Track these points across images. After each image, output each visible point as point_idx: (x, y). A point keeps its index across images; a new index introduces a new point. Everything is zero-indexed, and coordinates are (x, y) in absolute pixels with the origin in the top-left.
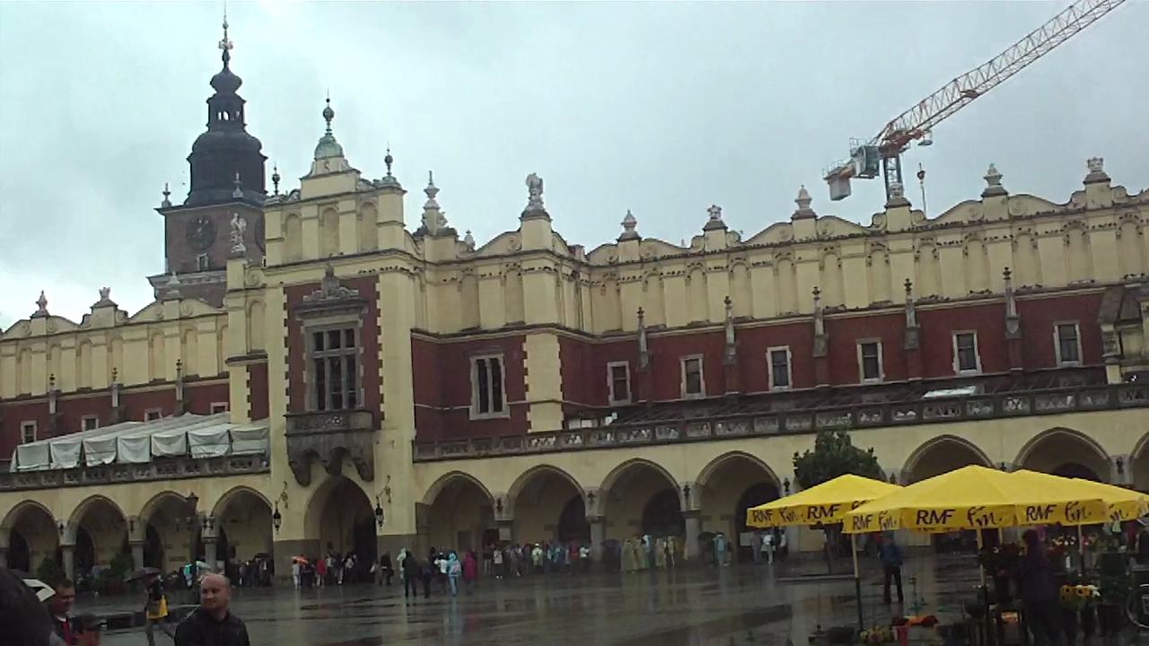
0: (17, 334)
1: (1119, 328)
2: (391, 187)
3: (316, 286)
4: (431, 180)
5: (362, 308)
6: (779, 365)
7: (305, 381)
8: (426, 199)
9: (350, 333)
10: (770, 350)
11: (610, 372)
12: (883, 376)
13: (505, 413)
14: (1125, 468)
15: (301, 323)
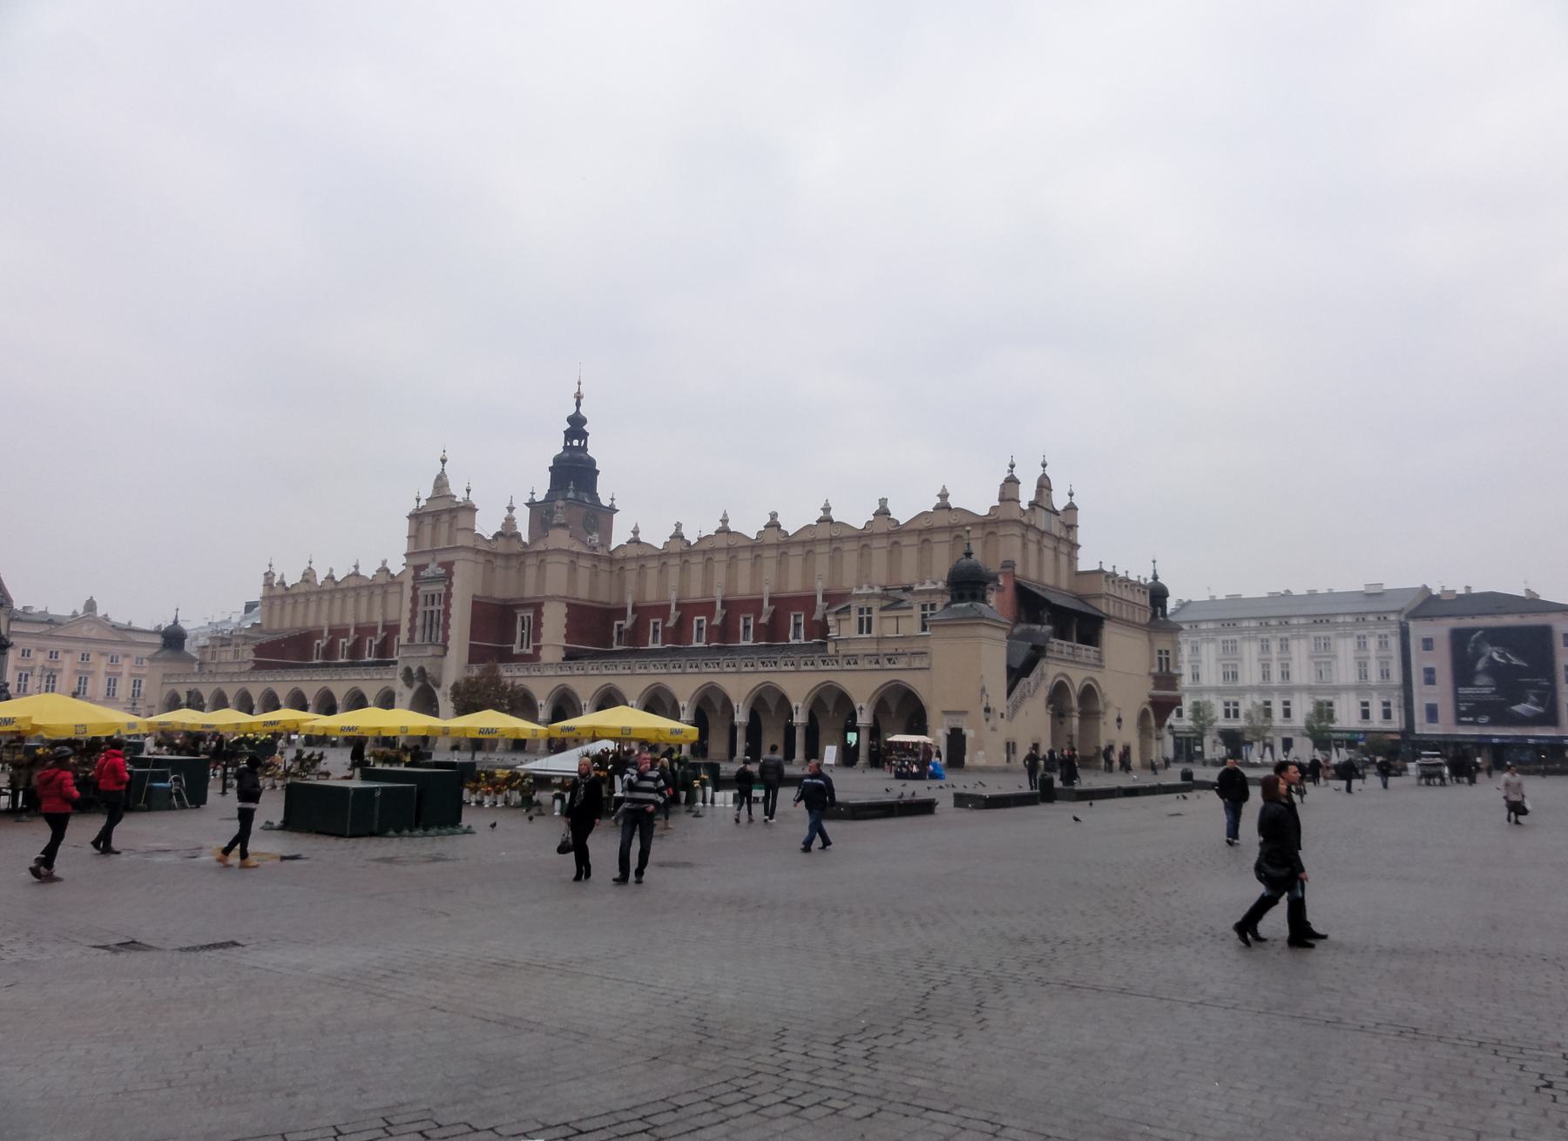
0: (344, 585)
1: (841, 617)
2: (470, 509)
3: (424, 567)
4: (511, 501)
5: (445, 581)
6: (700, 629)
7: (417, 624)
8: (506, 513)
9: (440, 595)
10: (696, 618)
11: (615, 627)
12: (752, 639)
13: (530, 651)
14: (799, 711)
15: (418, 588)
